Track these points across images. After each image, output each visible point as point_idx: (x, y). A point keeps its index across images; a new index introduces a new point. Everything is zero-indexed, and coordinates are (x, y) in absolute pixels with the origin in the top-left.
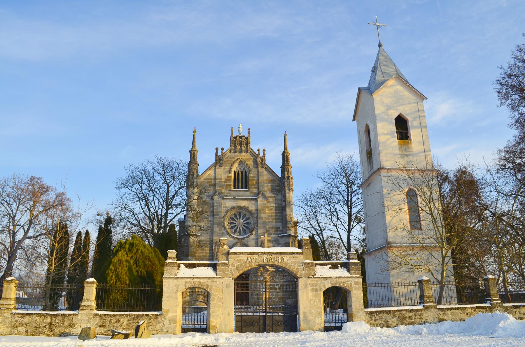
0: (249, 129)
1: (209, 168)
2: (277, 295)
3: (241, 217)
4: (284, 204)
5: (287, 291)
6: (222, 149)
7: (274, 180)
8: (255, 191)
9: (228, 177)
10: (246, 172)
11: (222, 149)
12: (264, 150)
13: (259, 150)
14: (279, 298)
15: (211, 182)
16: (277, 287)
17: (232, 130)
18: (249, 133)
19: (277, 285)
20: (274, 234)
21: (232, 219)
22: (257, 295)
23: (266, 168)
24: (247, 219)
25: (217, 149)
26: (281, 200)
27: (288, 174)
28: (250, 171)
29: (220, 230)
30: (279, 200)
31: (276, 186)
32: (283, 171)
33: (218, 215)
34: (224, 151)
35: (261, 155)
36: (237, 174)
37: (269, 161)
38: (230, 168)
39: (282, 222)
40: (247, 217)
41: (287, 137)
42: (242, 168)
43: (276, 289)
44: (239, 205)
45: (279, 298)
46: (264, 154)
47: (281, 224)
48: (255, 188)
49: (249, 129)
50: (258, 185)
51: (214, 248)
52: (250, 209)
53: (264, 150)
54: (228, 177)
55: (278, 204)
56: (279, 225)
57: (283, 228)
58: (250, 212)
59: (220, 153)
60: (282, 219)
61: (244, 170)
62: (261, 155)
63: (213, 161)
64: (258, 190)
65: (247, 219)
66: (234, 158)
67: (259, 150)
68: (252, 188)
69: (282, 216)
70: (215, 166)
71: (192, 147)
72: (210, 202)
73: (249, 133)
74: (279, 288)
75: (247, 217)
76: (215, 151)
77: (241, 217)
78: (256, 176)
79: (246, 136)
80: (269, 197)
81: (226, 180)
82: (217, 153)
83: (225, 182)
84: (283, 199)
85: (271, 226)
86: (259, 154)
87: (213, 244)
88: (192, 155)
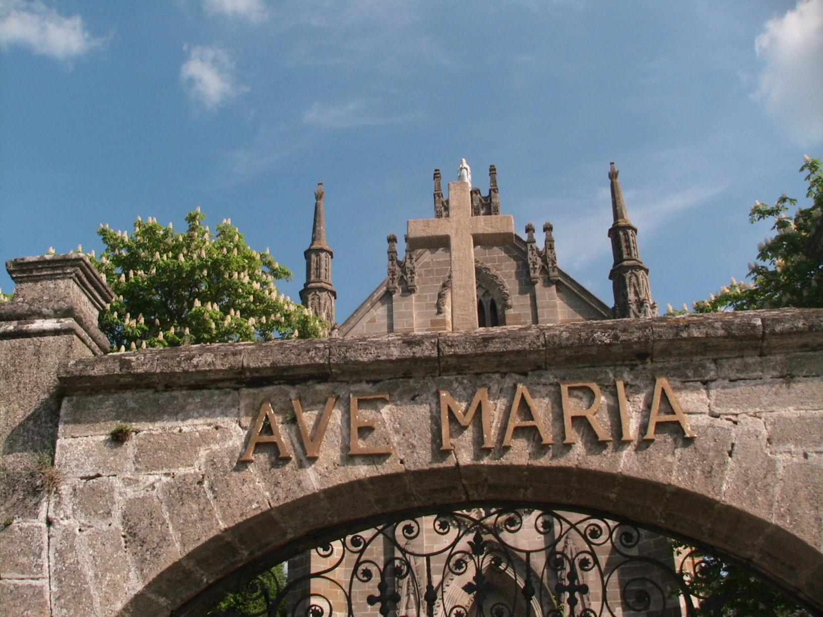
0: (492, 170)
1: (371, 302)
9: (433, 323)
12: (548, 229)
13: (529, 229)
17: (437, 175)
18: (494, 181)
23: (558, 283)
25: (392, 240)
27: (637, 294)
35: (540, 244)
38: (441, 296)
41: (618, 180)
49: (492, 170)
53: (548, 229)
62: (540, 244)
63: (384, 275)
67: (529, 229)
70: (387, 296)
71: (314, 239)
73: (494, 181)
76: (387, 246)
79: (485, 193)
88: (313, 265)
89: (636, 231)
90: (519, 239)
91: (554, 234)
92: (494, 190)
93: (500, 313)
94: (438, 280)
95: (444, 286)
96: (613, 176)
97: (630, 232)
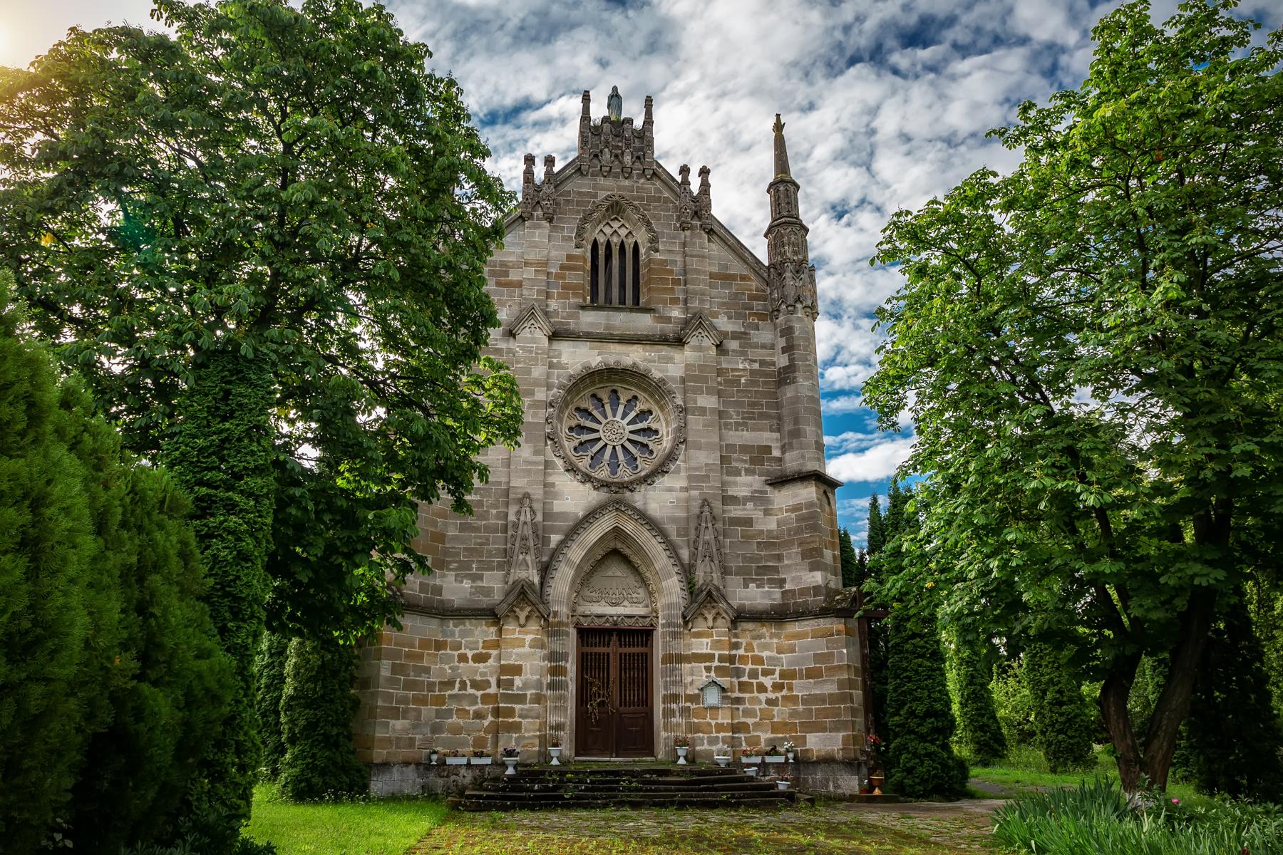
2: (766, 715)
3: (621, 408)
4: (783, 361)
5: (807, 700)
6: (549, 161)
7: (743, 278)
8: (676, 313)
9: (569, 257)
10: (636, 245)
11: (549, 161)
12: (704, 172)
13: (685, 170)
14: (775, 727)
15: (506, 274)
16: (767, 681)
19: (766, 673)
20: (749, 472)
21: (586, 413)
22: (685, 712)
24: (644, 414)
26: (772, 347)
28: (654, 240)
29: (536, 453)
30: (763, 346)
31: (752, 298)
32: (774, 248)
33: (532, 393)
34: (556, 169)
35: (695, 186)
36: (602, 252)
37: (720, 210)
39: (779, 430)
40: (640, 406)
42: (623, 232)
43: (762, 688)
44: (611, 361)
45: (775, 727)
46: (705, 186)
47: (776, 435)
48: (674, 301)
50: (686, 292)
51: (512, 518)
52: (656, 374)
53: (704, 172)
54: (569, 257)
55: (762, 363)
56: (767, 437)
57: (783, 449)
58: (658, 390)
59: (539, 171)
60: (780, 418)
61: (631, 241)
62: (695, 186)
64: (687, 309)
65: (644, 414)
66: (595, 196)
67: (685, 170)
68: (664, 302)
69: (778, 406)
72: (503, 345)
74: (777, 687)
75: (640, 406)
77: (621, 408)
78: (679, 258)
79: (638, 123)
80: (725, 335)
81: (562, 267)
82: (529, 175)
83: (558, 276)
84: (782, 342)
85: (738, 442)
86: (686, 182)
87: (507, 505)
89: (798, 187)
90: (674, 180)
91: (711, 179)
92: (649, 121)
93: (643, 257)
94: (578, 212)
95: (585, 220)
96: (779, 127)
97: (792, 188)
